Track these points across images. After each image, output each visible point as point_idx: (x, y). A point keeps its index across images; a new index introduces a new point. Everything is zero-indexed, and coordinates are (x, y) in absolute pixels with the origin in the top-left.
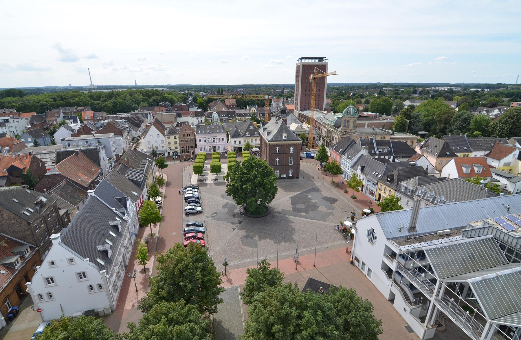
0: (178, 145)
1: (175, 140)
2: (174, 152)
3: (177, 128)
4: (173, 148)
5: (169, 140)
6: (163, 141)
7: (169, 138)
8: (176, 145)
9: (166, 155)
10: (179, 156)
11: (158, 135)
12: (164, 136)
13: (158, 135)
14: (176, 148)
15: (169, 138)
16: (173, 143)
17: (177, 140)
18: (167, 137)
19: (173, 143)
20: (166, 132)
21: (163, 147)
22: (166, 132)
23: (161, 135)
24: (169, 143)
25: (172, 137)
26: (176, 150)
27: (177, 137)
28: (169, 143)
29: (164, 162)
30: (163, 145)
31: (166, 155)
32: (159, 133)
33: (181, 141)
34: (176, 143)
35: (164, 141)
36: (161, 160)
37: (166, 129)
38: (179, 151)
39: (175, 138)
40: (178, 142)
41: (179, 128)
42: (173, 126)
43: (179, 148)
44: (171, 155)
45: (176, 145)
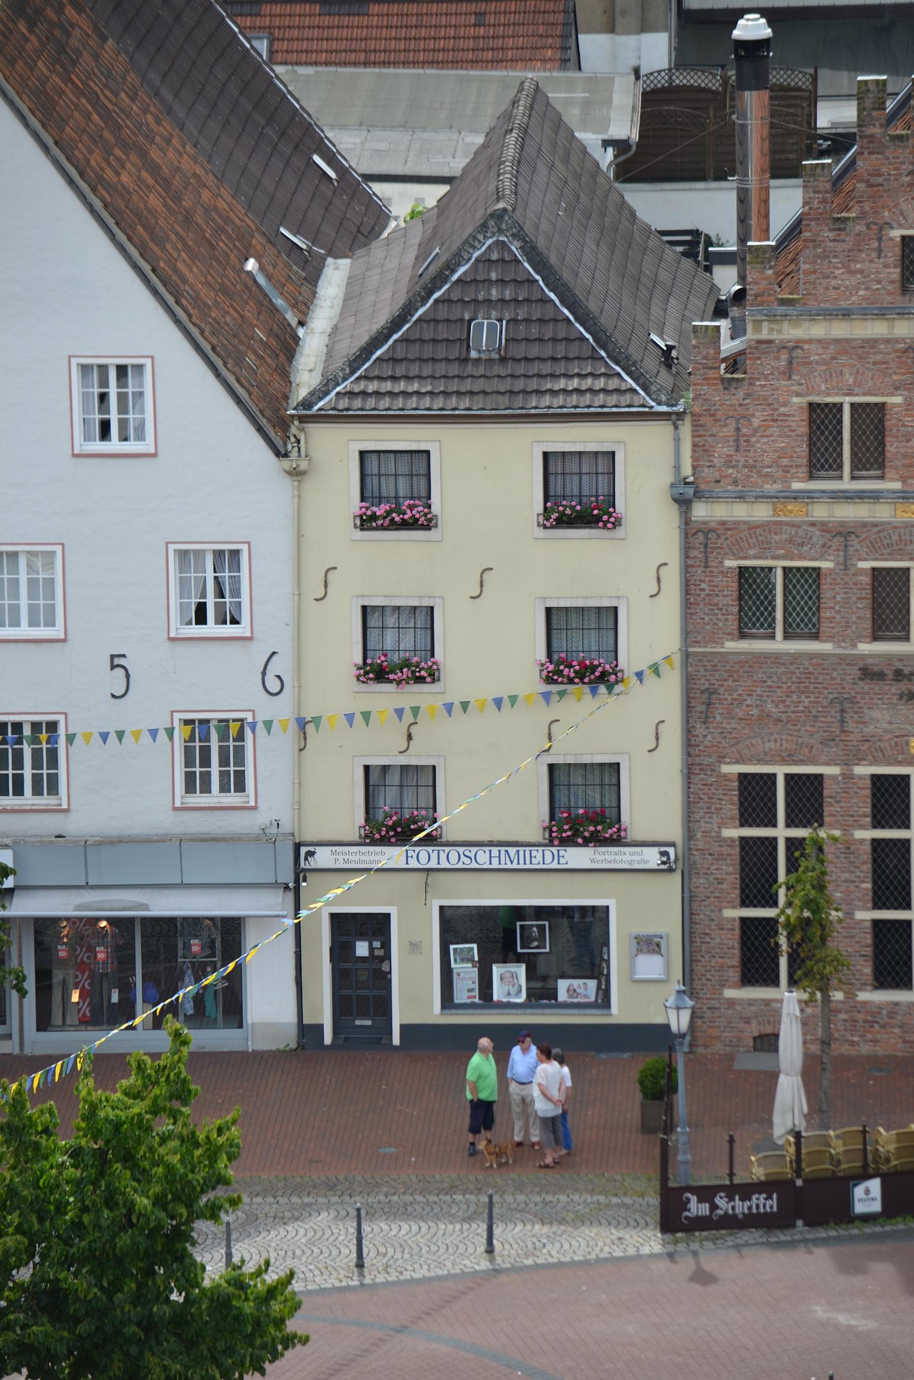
0: (637, 733)
1: (580, 567)
2: (494, 934)
3: (664, 207)
4: (491, 795)
5: (395, 568)
6: (213, 594)
7: (396, 502)
8: (589, 727)
9: (277, 994)
10: (650, 1064)
11: (111, 397)
12: (277, 421)
13: (111, 397)
14: (583, 808)
15: (396, 502)
16: (491, 646)
17: (635, 572)
18: (337, 451)
19: (491, 646)
20: (335, 311)
21: (213, 751)
22: (335, 311)
23: (186, 392)
24: (397, 652)
25: (487, 471)
26: (570, 878)
27: (645, 461)
28: (397, 652)
29: (192, 1195)
30: (219, 681)
31: (277, 994)
32: (133, 322)
33: (749, 595)
34: (580, 651)
35: (264, 587)
36: (117, 1147)
37: (352, 216)
38: (638, 899)
39: (578, 502)
40: (651, 633)
41: (710, 208)
42: (539, 130)
43: (653, 802)
44: (415, 994)
45: (589, 727)
